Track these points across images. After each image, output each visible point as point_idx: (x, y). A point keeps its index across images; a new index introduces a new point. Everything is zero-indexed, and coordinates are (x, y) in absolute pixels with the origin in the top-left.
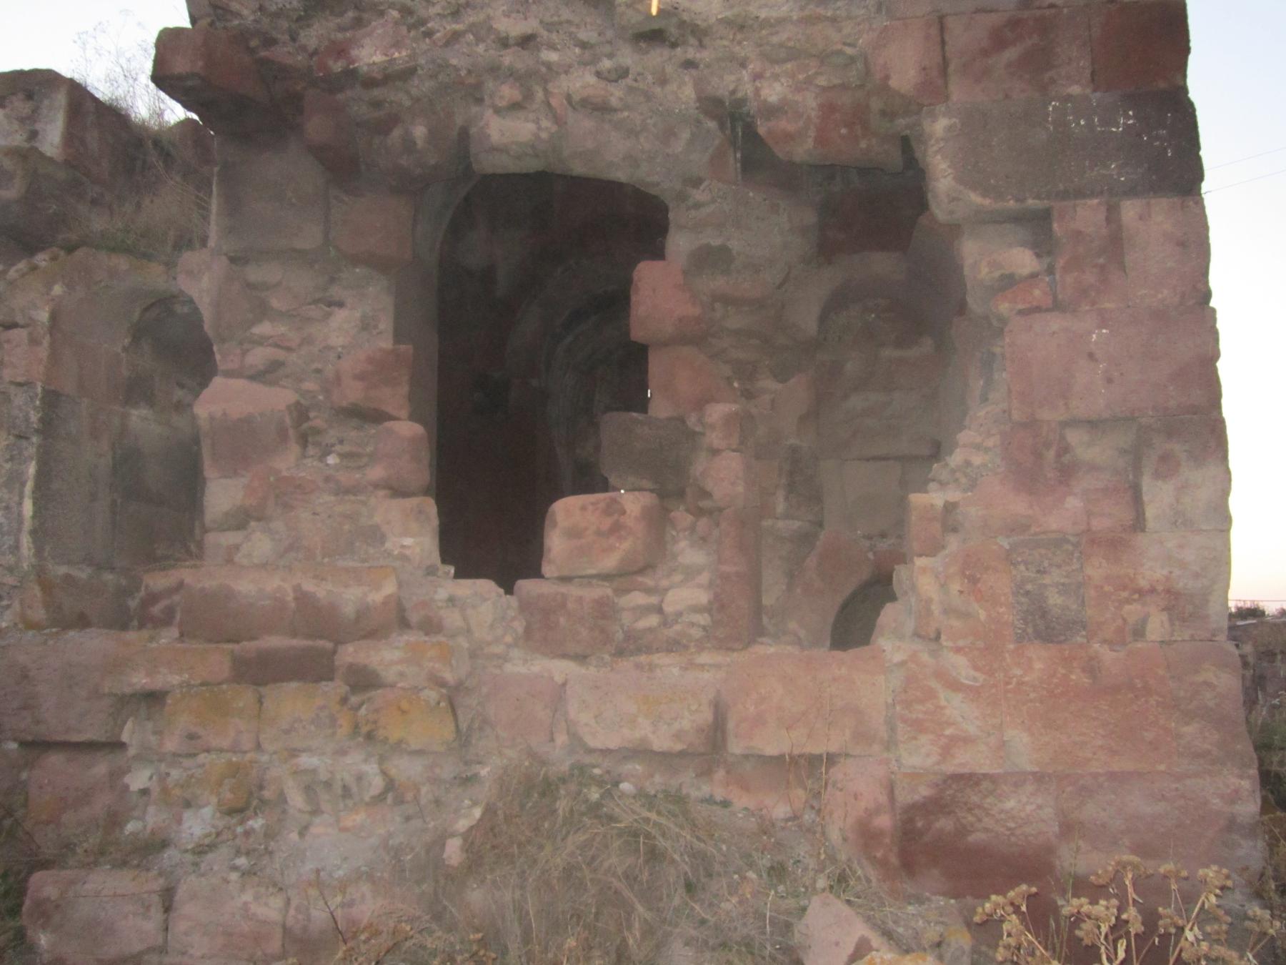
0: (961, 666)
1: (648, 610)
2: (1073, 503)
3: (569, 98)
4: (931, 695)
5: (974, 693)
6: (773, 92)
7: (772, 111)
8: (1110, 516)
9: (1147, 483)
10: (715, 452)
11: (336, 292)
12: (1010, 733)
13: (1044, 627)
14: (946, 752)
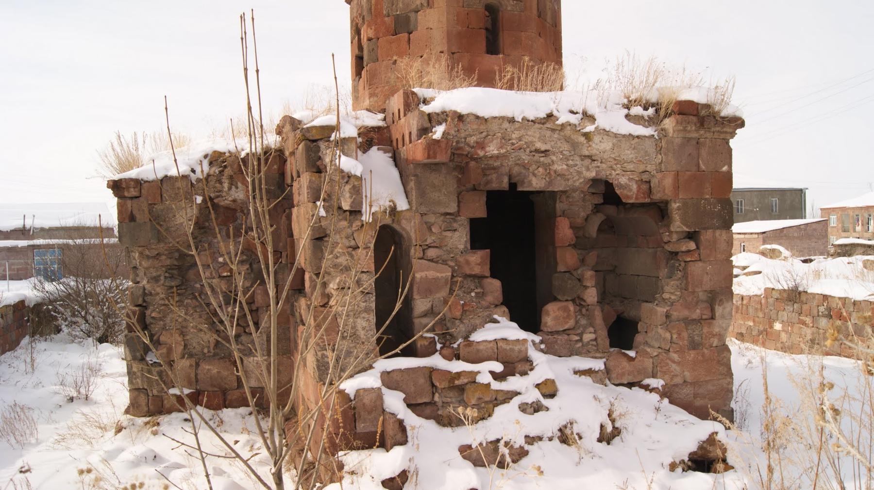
0: (675, 356)
1: (577, 341)
2: (698, 311)
3: (555, 172)
4: (667, 364)
5: (678, 363)
6: (623, 180)
7: (621, 186)
8: (707, 314)
9: (717, 307)
10: (586, 287)
11: (455, 225)
12: (686, 373)
13: (694, 345)
14: (672, 379)
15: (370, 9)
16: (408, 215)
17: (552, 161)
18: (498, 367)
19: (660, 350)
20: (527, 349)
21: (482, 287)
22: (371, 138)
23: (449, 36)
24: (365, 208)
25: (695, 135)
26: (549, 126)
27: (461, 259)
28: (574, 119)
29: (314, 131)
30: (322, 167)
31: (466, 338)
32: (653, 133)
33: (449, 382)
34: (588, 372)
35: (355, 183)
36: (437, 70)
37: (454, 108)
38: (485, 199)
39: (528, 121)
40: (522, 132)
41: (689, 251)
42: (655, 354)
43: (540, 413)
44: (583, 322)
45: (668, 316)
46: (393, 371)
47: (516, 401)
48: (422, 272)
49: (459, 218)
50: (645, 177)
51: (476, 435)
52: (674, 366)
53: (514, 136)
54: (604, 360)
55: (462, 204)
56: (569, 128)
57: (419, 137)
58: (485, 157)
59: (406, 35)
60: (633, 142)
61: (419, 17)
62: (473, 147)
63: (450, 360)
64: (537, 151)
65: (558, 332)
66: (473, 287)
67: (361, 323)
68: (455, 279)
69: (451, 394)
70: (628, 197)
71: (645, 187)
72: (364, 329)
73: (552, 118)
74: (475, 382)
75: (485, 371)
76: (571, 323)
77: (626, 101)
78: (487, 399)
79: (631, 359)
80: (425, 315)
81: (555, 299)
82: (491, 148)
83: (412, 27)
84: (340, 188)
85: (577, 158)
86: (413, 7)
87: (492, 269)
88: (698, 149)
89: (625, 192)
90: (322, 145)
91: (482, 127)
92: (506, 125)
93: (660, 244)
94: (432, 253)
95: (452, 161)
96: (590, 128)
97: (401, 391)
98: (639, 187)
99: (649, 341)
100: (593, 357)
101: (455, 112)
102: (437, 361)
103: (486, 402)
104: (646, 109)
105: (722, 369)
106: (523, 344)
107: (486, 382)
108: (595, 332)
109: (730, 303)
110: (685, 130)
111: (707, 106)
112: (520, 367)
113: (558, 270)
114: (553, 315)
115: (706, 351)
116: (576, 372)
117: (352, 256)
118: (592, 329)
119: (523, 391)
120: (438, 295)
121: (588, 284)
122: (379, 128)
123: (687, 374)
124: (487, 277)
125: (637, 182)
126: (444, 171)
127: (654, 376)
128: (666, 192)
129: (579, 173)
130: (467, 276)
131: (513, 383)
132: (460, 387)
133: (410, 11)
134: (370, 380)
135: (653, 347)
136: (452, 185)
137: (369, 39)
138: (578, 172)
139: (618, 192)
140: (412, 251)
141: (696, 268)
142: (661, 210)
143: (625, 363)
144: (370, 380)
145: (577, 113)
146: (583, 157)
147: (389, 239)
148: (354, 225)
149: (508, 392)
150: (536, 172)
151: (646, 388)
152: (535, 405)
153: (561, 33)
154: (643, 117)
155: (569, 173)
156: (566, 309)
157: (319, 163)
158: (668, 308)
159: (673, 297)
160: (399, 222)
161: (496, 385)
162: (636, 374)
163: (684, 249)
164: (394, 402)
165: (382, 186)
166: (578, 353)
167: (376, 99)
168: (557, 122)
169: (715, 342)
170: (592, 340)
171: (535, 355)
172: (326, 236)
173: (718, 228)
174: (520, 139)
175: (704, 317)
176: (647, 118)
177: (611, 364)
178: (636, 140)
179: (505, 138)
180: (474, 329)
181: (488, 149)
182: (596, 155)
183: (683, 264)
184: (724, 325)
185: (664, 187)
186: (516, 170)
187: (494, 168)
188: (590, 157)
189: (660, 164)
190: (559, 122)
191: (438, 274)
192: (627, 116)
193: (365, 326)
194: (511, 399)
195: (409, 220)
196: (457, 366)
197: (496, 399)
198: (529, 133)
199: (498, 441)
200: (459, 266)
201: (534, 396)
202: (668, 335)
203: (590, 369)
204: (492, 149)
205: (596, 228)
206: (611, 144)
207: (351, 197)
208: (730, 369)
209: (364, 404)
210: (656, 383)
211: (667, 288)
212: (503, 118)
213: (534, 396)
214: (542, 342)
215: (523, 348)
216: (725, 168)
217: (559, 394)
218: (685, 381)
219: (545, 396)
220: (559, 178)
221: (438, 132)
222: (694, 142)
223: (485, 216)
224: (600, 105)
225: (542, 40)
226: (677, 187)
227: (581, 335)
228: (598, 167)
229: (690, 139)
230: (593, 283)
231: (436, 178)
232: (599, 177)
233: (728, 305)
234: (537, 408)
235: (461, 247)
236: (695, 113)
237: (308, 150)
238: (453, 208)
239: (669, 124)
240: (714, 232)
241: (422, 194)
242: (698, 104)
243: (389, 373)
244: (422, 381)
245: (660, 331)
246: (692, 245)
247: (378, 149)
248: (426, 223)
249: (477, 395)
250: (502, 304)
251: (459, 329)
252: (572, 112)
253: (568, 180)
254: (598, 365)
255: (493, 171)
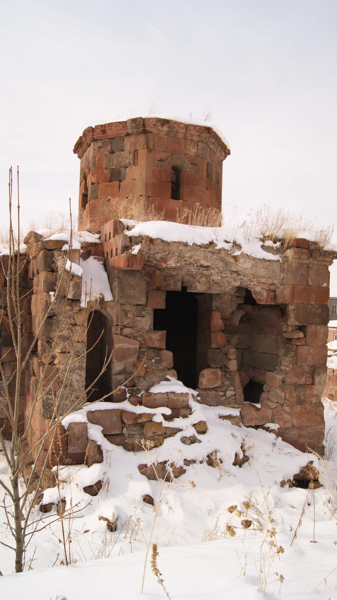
0: (287, 409)
1: (222, 396)
2: (304, 379)
3: (213, 281)
4: (282, 414)
5: (289, 414)
6: (258, 289)
7: (256, 293)
8: (309, 381)
9: (316, 377)
10: (230, 359)
11: (144, 313)
13: (300, 402)
14: (284, 424)
15: (95, 163)
16: (112, 304)
17: (212, 274)
18: (168, 411)
19: (277, 404)
20: (188, 400)
21: (159, 356)
22: (89, 251)
23: (147, 186)
24: (83, 297)
25: (306, 262)
26: (210, 250)
27: (147, 336)
28: (227, 246)
29: (51, 244)
30: (55, 268)
31: (147, 390)
32: (279, 259)
33: (134, 420)
34: (229, 417)
35: (77, 281)
36: (137, 208)
37: (147, 234)
38: (165, 296)
39: (197, 246)
40: (192, 253)
41: (299, 338)
42: (274, 406)
43: (195, 444)
44: (227, 383)
45: (283, 381)
46: (96, 411)
47: (179, 435)
48: (120, 344)
49: (146, 308)
50: (272, 288)
51: (150, 457)
52: (286, 415)
53: (186, 255)
54: (240, 409)
55: (149, 299)
56: (223, 252)
57: (123, 252)
58: (167, 268)
59: (118, 182)
60: (265, 264)
61: (127, 171)
62: (158, 261)
63: (135, 405)
64: (202, 266)
65: (209, 389)
66: (154, 356)
67: (75, 377)
68: (142, 350)
69: (135, 429)
70: (261, 300)
71: (272, 294)
72: (77, 381)
73: (213, 245)
74: (151, 421)
75: (159, 414)
76: (219, 383)
77: (262, 236)
78: (160, 433)
79: (258, 409)
80: (120, 373)
81: (209, 367)
82: (171, 262)
83: (122, 178)
84: (67, 283)
85: (228, 273)
86: (124, 164)
87: (167, 344)
88: (308, 271)
89: (259, 297)
90: (56, 253)
91: (166, 248)
92: (181, 247)
93: (280, 333)
94: (127, 331)
95: (144, 269)
96: (237, 253)
97: (100, 425)
98: (268, 294)
99: (271, 397)
100: (232, 407)
101: (148, 237)
102: (126, 406)
103: (159, 435)
104: (275, 242)
105: (318, 418)
106: (186, 397)
107: (159, 421)
108: (235, 390)
109: (325, 375)
110: (300, 258)
111: (315, 243)
112: (183, 412)
113: (212, 347)
114: (206, 377)
115: (308, 406)
116: (220, 417)
117: (72, 331)
118: (232, 388)
119: (184, 428)
120: (129, 360)
121: (231, 357)
122: (95, 244)
123: (295, 421)
124: (163, 349)
125: (267, 290)
126: (138, 275)
127: (273, 422)
128: (286, 298)
129: (229, 282)
130: (150, 348)
131: (178, 423)
132: (141, 424)
133: (122, 167)
134: (78, 417)
135: (273, 402)
136: (143, 286)
137: (93, 184)
138: (228, 281)
139: (254, 296)
140: (114, 329)
141: (303, 350)
142: (281, 310)
143: (254, 412)
144: (78, 417)
145: (229, 242)
146: (232, 272)
147: (98, 321)
148: (75, 309)
149: (174, 429)
150: (200, 280)
151: (267, 429)
152: (192, 439)
153: (221, 188)
154: (272, 248)
155: (221, 282)
156: (216, 374)
157: (53, 265)
158: (284, 376)
159: (287, 369)
160: (105, 309)
161: (166, 424)
162: (261, 419)
163: (296, 337)
164: (95, 433)
165: (94, 283)
166: (223, 404)
167: (94, 224)
168: (216, 248)
169: (314, 400)
170: (232, 396)
171: (193, 404)
172: (54, 316)
173: (319, 324)
174: (190, 257)
175: (307, 383)
176: (275, 249)
177: (244, 412)
178: (268, 263)
179: (181, 256)
180: (153, 385)
181: (168, 263)
182: (240, 271)
183: (295, 347)
184: (320, 389)
185: (285, 295)
186: (187, 278)
187: (172, 276)
188: (236, 272)
189: (283, 279)
190: (217, 248)
191: (130, 346)
192: (262, 247)
193: (78, 378)
194: (176, 433)
195: (112, 308)
196: (140, 410)
197: (165, 433)
198: (197, 254)
199: (165, 462)
200: (145, 341)
201: (191, 432)
202: (283, 394)
203: (230, 415)
204: (172, 263)
205: (238, 319)
206: (251, 265)
207: (73, 290)
208: (323, 419)
209: (74, 433)
210: (274, 426)
211: (284, 363)
212: (180, 243)
213: (191, 432)
214: (198, 395)
215: (186, 399)
216: (325, 285)
217: (209, 431)
218: (293, 426)
219: (199, 432)
220: (215, 285)
221: (136, 249)
222: (305, 267)
223: (165, 308)
224: (245, 238)
225: (209, 192)
226: (293, 295)
227: (225, 392)
228: (242, 279)
229: (303, 264)
230: (235, 357)
231: (132, 281)
232: (242, 286)
233: (323, 376)
234: (193, 440)
235: (147, 328)
236: (307, 247)
237: (46, 256)
238: (143, 301)
239: (289, 253)
240: (316, 327)
241: (122, 290)
242: (309, 241)
243: (92, 412)
244: (115, 419)
245: (278, 391)
246: (301, 335)
247: (94, 258)
248: (124, 310)
249: (153, 430)
250: (172, 368)
251: (142, 384)
252: (226, 242)
253: (221, 287)
254: (236, 412)
255: (171, 278)
